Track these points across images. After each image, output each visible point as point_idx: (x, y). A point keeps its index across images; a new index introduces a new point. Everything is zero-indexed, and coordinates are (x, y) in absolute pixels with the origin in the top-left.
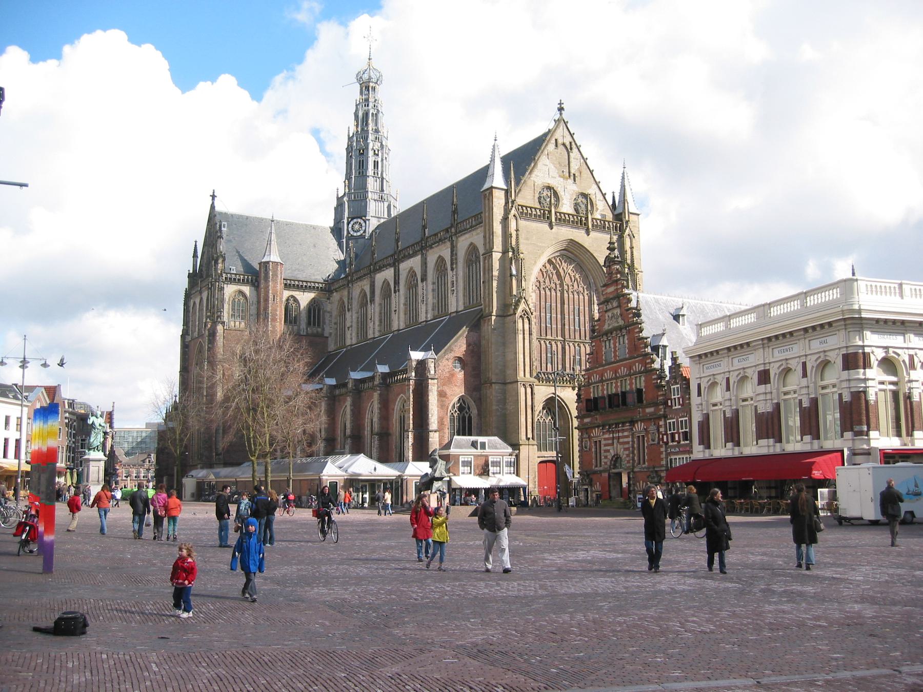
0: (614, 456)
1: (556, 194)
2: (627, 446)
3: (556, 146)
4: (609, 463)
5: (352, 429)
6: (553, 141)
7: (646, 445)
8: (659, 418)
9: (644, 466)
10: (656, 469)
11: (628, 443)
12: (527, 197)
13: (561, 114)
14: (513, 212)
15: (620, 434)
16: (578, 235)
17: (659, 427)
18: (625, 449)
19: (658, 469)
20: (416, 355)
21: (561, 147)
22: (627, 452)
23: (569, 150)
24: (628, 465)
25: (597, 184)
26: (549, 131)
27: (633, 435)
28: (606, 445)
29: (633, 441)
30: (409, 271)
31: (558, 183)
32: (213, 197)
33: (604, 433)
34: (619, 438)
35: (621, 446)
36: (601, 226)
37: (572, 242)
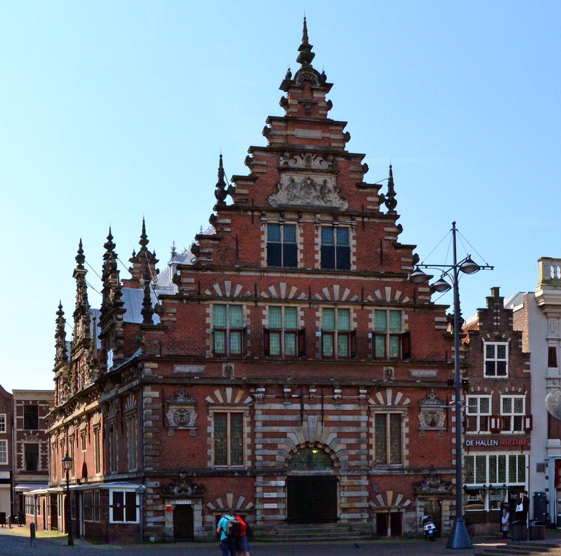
2: (352, 429)
4: (280, 458)
7: (405, 430)
9: (398, 466)
10: (439, 472)
11: (357, 424)
15: (328, 407)
18: (341, 435)
19: (443, 472)
22: (352, 441)
24: (353, 463)
27: (369, 413)
29: (369, 424)
33: (264, 401)
34: (323, 412)
35: (331, 429)
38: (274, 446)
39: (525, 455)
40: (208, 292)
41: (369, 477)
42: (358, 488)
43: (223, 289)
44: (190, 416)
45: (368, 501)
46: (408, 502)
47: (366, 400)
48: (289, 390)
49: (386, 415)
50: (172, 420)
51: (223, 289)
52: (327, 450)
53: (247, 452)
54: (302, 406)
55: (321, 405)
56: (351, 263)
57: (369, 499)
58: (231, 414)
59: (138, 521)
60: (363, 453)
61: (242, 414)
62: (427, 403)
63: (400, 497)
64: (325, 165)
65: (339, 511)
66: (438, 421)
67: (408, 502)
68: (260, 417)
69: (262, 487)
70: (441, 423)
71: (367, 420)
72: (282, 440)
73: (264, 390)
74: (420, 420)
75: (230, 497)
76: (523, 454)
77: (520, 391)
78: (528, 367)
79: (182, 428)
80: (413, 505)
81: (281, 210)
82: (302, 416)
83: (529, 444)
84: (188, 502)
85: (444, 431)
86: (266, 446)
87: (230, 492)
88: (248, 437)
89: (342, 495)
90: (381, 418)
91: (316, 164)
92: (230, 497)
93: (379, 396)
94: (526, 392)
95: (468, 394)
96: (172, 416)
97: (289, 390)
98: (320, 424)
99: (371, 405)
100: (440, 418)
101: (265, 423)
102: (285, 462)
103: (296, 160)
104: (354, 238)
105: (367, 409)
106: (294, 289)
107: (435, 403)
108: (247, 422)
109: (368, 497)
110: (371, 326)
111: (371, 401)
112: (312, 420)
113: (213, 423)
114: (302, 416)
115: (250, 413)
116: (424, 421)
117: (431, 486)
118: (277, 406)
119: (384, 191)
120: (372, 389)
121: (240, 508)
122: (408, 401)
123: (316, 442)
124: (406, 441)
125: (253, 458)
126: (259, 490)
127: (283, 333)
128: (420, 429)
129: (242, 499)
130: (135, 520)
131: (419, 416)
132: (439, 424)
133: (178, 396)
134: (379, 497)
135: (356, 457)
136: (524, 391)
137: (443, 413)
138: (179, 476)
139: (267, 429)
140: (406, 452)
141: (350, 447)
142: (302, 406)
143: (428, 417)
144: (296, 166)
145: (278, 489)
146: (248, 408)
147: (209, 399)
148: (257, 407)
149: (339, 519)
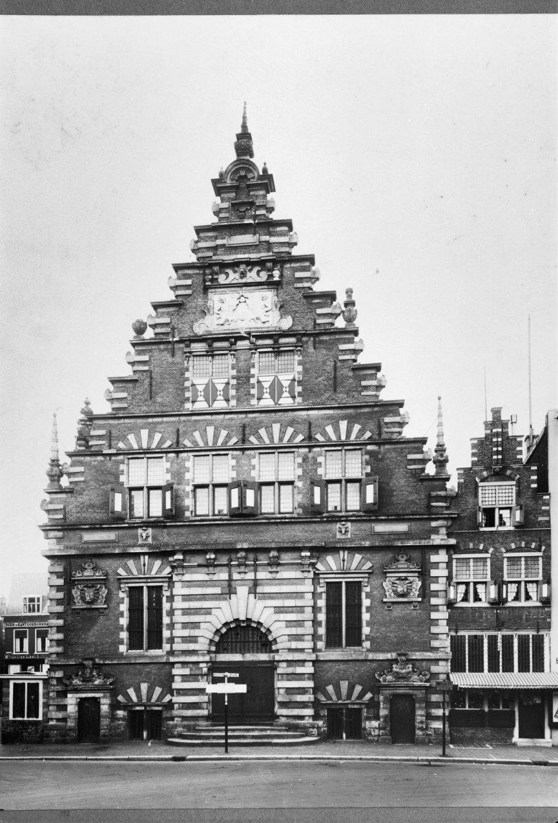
0: (226, 624)
11: (300, 595)
18: (279, 610)
29: (315, 595)
34: (256, 583)
38: (196, 625)
39: (543, 635)
40: (121, 445)
41: (315, 662)
42: (300, 677)
43: (139, 441)
44: (98, 593)
45: (314, 693)
46: (369, 696)
47: (313, 565)
48: (213, 556)
49: (341, 582)
50: (79, 598)
51: (139, 441)
52: (263, 630)
53: (166, 634)
54: (230, 575)
55: (253, 573)
56: (296, 394)
57: (315, 690)
58: (148, 587)
59: (40, 718)
60: (307, 632)
61: (161, 587)
62: (394, 567)
63: (358, 688)
64: (264, 276)
65: (277, 706)
66: (411, 590)
67: (369, 696)
68: (179, 590)
69: (182, 675)
70: (415, 596)
71: (312, 591)
72: (208, 618)
73: (180, 557)
74: (386, 588)
75: (144, 687)
76: (541, 633)
77: (533, 547)
78: (548, 513)
79: (89, 606)
80: (376, 700)
81: (209, 340)
82: (230, 586)
83: (548, 620)
84: (97, 695)
85: (419, 602)
86: (185, 625)
87: (144, 682)
88: (167, 615)
89: (279, 686)
90: (333, 588)
91: (252, 276)
92: (144, 687)
93: (330, 559)
94: (543, 548)
95: (455, 553)
96: (79, 593)
97: (213, 556)
98: (252, 596)
99: (318, 570)
100: (414, 586)
101: (187, 598)
102: (210, 645)
103: (227, 274)
104: (299, 364)
105: (313, 577)
106: (224, 433)
107: (406, 566)
108: (167, 597)
109: (313, 688)
110: (320, 471)
111: (319, 566)
112: (242, 591)
113: (127, 600)
114: (230, 586)
115: (169, 587)
116: (391, 591)
117: (398, 676)
118: (200, 576)
119: (341, 299)
120: (320, 551)
121: (156, 701)
122: (369, 565)
123: (247, 619)
124: (366, 617)
125: (171, 640)
126: (177, 679)
127: (343, 482)
128: (385, 600)
129: (158, 690)
130: (37, 717)
131: (384, 584)
132: (412, 594)
133: (86, 569)
134: (330, 688)
135: (298, 637)
136: (540, 547)
137: (417, 579)
138: (83, 665)
139: (186, 605)
140: (366, 630)
141: (289, 623)
142: (230, 575)
143: (396, 585)
144: (228, 282)
145: (200, 677)
146: (167, 580)
147: (121, 571)
148: (175, 578)
149: (278, 717)
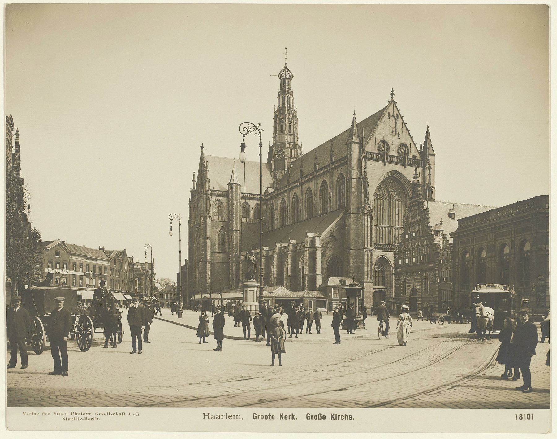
0: (413, 288)
1: (387, 144)
3: (389, 116)
5: (278, 274)
6: (387, 114)
8: (436, 270)
12: (371, 147)
13: (392, 98)
14: (363, 155)
16: (399, 168)
17: (436, 274)
20: (310, 235)
21: (392, 118)
23: (396, 119)
25: (412, 138)
26: (385, 107)
28: (408, 283)
29: (422, 281)
30: (308, 189)
31: (389, 139)
32: (202, 147)
36: (414, 163)
37: (396, 172)
